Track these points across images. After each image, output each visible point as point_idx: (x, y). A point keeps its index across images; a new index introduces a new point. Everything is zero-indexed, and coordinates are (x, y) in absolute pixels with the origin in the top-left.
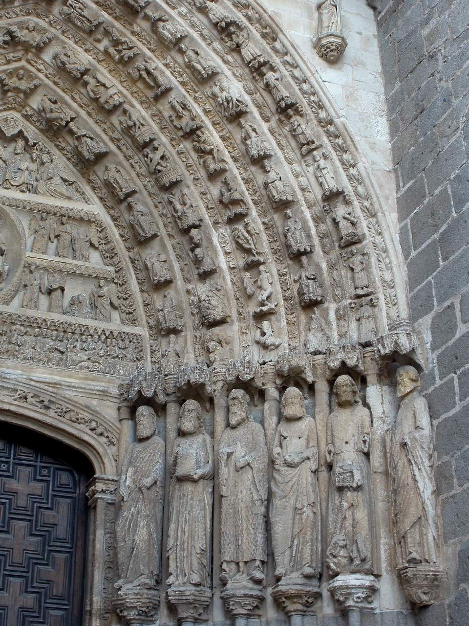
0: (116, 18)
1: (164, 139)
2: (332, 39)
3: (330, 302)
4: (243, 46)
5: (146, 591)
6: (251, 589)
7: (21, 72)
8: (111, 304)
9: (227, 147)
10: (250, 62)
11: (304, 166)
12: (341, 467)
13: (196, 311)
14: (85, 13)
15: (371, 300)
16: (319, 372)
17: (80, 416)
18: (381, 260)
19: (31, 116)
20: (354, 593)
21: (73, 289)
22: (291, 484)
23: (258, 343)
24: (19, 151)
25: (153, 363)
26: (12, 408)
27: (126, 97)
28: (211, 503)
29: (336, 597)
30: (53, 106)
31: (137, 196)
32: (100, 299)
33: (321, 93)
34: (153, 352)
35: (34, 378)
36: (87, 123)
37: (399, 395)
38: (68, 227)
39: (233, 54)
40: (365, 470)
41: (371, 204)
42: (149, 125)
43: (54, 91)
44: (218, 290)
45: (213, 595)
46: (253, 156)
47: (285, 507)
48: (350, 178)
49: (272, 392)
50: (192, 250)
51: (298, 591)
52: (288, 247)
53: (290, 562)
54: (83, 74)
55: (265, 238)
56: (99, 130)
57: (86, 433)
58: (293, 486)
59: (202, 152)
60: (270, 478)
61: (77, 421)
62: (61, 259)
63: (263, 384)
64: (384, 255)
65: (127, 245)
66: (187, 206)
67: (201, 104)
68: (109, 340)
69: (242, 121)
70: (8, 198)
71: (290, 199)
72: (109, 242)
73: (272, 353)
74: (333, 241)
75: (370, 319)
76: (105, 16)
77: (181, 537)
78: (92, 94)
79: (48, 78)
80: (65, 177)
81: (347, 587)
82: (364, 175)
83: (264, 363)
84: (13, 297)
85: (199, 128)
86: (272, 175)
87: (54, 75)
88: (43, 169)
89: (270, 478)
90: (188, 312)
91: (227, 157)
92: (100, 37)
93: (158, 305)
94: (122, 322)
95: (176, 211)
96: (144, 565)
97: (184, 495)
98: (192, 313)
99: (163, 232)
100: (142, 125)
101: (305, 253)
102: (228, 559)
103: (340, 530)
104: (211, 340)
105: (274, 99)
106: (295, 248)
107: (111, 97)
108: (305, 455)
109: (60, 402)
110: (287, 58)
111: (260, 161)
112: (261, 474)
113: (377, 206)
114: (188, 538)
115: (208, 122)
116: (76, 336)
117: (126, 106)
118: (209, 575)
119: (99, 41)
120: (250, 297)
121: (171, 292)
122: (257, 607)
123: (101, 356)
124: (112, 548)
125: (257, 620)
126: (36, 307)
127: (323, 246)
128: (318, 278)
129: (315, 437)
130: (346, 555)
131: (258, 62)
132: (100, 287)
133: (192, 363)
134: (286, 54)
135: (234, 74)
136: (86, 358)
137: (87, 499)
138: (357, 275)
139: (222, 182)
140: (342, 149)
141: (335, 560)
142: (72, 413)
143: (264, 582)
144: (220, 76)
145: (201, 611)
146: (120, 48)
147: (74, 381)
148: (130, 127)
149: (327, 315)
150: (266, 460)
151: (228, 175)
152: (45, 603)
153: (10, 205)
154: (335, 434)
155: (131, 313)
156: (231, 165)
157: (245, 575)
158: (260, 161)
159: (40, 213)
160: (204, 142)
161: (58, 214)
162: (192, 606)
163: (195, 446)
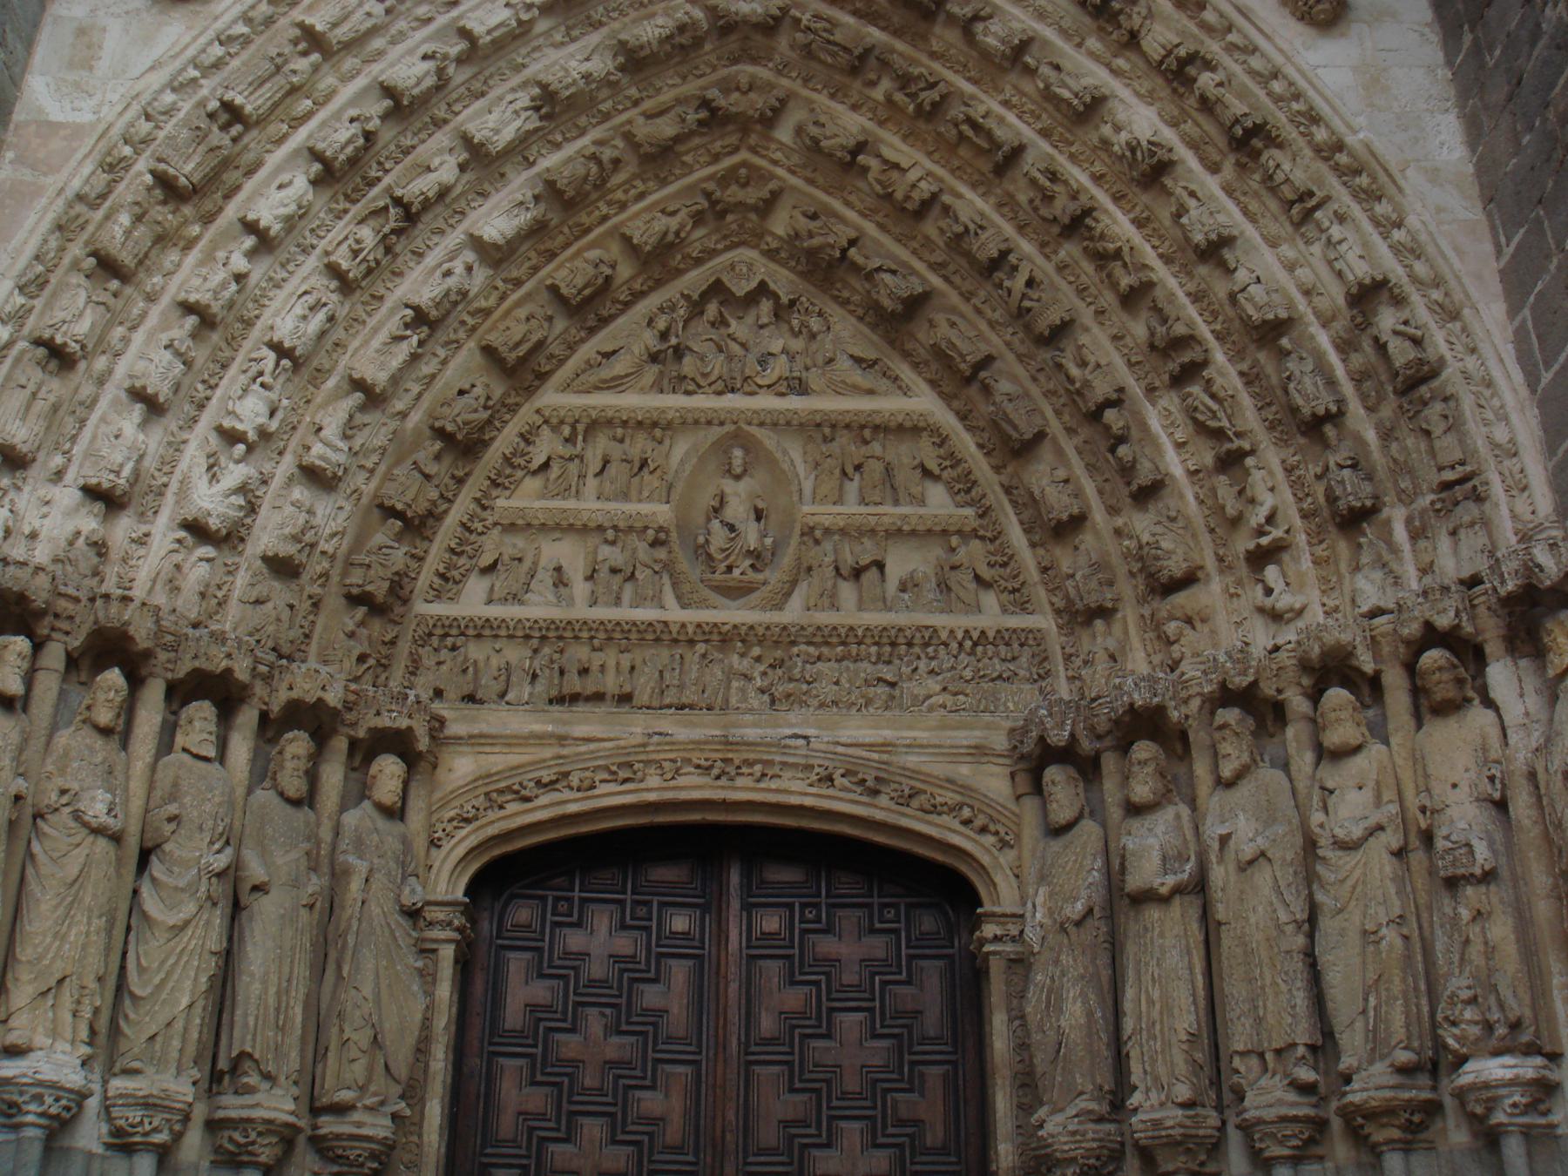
0: (897, 33)
1: (1026, 247)
3: (1392, 506)
4: (1143, 33)
5: (1091, 1126)
6: (1293, 1105)
7: (743, 171)
8: (977, 578)
9: (1147, 238)
10: (1161, 62)
11: (1301, 246)
12: (1447, 838)
13: (1136, 567)
14: (838, 37)
15: (1475, 488)
16: (1386, 649)
17: (939, 799)
18: (1483, 402)
19: (777, 250)
20: (1503, 1097)
21: (902, 562)
22: (1350, 883)
23: (1261, 610)
24: (765, 320)
25: (1071, 679)
26: (808, 801)
27: (941, 180)
28: (1201, 938)
29: (1469, 1108)
30: (813, 225)
31: (997, 365)
32: (953, 573)
33: (1311, 93)
34: (1068, 658)
35: (843, 740)
36: (882, 245)
37: (1551, 673)
38: (876, 447)
39: (1128, 54)
40: (1498, 837)
41: (1446, 294)
42: (994, 225)
43: (810, 196)
44: (1173, 520)
45: (1224, 1122)
46: (1197, 246)
47: (1342, 933)
48: (1397, 249)
49: (1297, 703)
50: (1113, 450)
51: (1387, 1100)
52: (1294, 410)
53: (1367, 1041)
55: (1246, 401)
56: (903, 254)
57: (954, 831)
58: (1354, 887)
59: (1104, 258)
60: (1310, 878)
61: (934, 810)
62: (872, 509)
63: (1279, 691)
64: (1487, 393)
65: (994, 461)
66: (1090, 368)
67: (1086, 165)
68: (980, 649)
69: (1168, 182)
70: (755, 412)
71: (1283, 314)
72: (959, 462)
73: (1292, 626)
74: (1382, 384)
75: (1477, 527)
76: (875, 34)
77: (1149, 1013)
78: (878, 188)
79: (793, 173)
80: (858, 352)
81: (1486, 1086)
82: (1423, 237)
83: (1276, 649)
84: (788, 595)
85: (1088, 212)
86: (1242, 276)
87: (804, 166)
88: (814, 346)
89: (1310, 878)
90: (1121, 570)
91: (1150, 256)
92: (872, 76)
93: (1065, 566)
94: (1004, 611)
95: (1071, 380)
96: (1082, 1075)
97: (1146, 929)
98: (1130, 572)
99: (1055, 427)
100: (981, 227)
101: (1329, 417)
102: (1240, 1047)
103: (1461, 966)
104: (1172, 618)
105: (1222, 125)
106: (1306, 411)
107: (914, 186)
108: (1372, 822)
109: (898, 778)
110: (1232, 37)
111: (1215, 251)
112: (1291, 870)
113: (1458, 296)
114: (1161, 1013)
115: (1102, 198)
116: (917, 650)
117: (946, 198)
118: (1211, 1083)
119: (873, 84)
120: (1236, 522)
121: (1087, 540)
122: (1311, 1141)
123: (967, 681)
124: (1023, 1046)
125: (1316, 1167)
126: (834, 606)
127: (1364, 397)
128: (1363, 463)
129: (1392, 781)
130: (1476, 1018)
131: (1178, 59)
132: (953, 550)
133: (1144, 669)
134: (1229, 29)
135: (1137, 94)
136: (938, 688)
137: (973, 956)
138: (1437, 444)
139: (1150, 308)
140: (1369, 196)
141: (1456, 1031)
142: (923, 797)
143: (1322, 1089)
144: (1111, 104)
145: (1203, 1157)
146: (913, 89)
147: (922, 735)
148: (959, 237)
149: (1390, 532)
150: (1299, 840)
151: (1158, 293)
152: (912, 1163)
153: (761, 424)
154: (1431, 770)
155: (1018, 590)
157: (1277, 1078)
158: (1215, 251)
159: (820, 429)
160: (1102, 237)
161: (855, 425)
162: (1181, 1149)
163: (1160, 829)
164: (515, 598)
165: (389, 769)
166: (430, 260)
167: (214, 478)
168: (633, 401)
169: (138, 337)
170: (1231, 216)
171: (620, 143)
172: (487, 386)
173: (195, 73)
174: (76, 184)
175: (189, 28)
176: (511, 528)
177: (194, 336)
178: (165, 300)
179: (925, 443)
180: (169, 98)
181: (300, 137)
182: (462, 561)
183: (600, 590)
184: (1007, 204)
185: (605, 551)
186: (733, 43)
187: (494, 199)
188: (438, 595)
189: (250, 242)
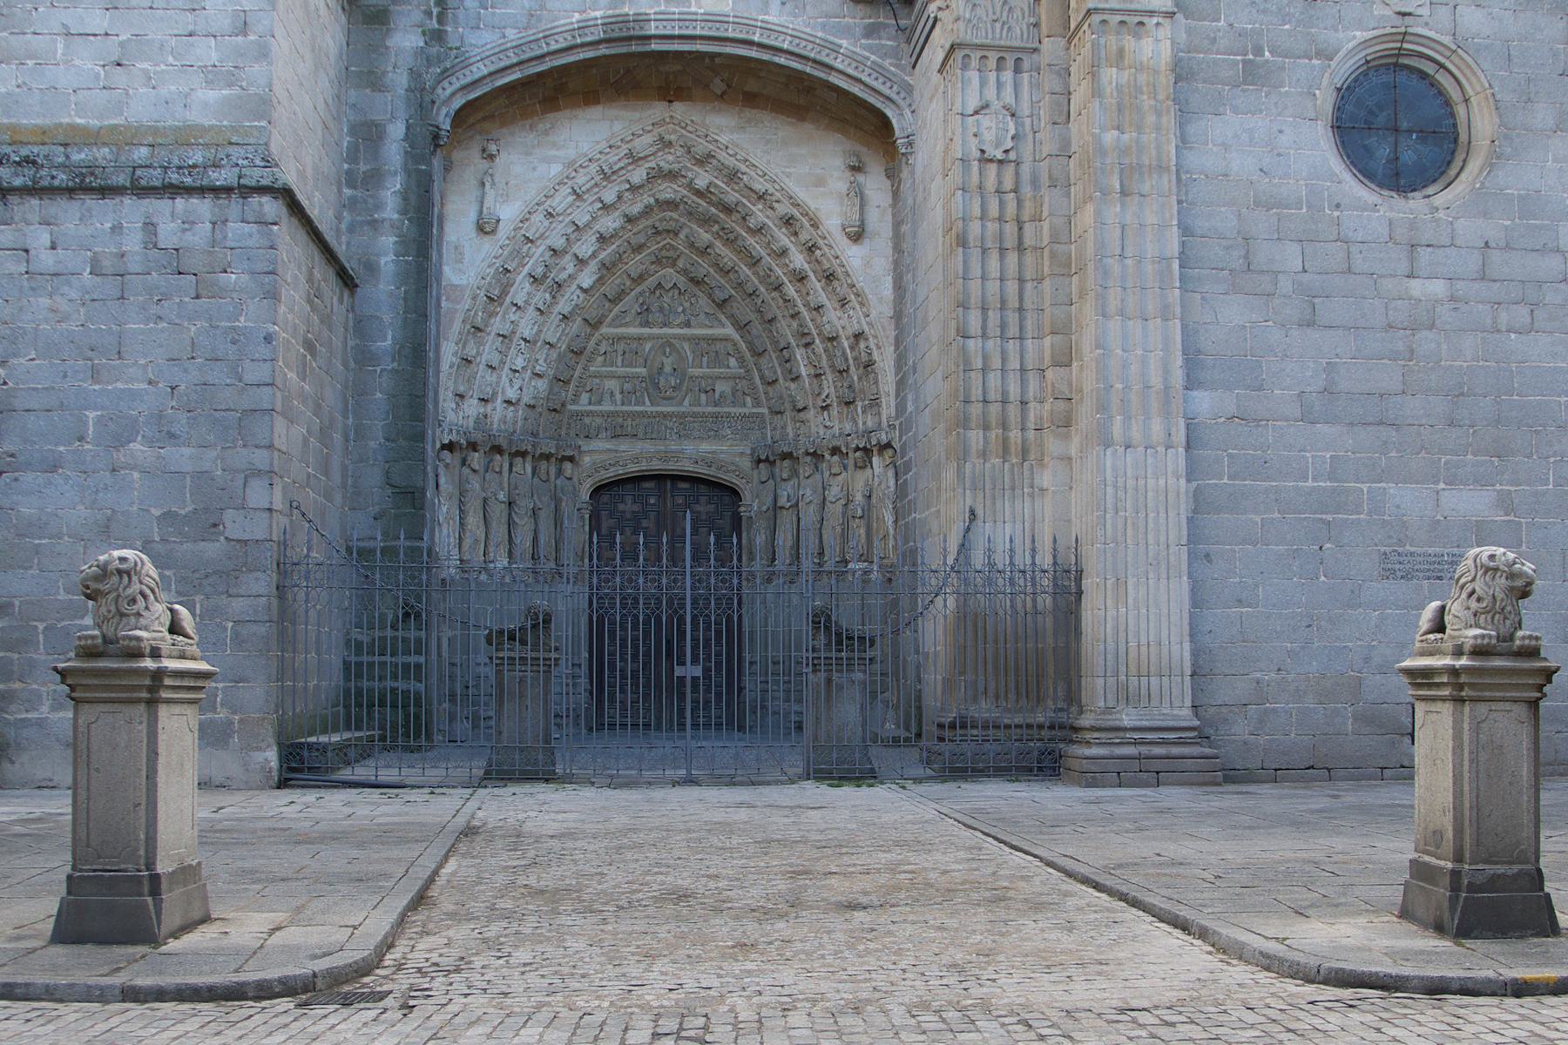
1: (762, 289)
2: (851, 229)
14: (700, 209)
21: (721, 387)
49: (827, 456)
55: (824, 356)
56: (723, 282)
86: (824, 318)
91: (799, 302)
93: (771, 393)
111: (818, 308)
140: (861, 304)
156: (802, 309)
158: (818, 308)
159: (695, 340)
164: (599, 403)
165: (568, 466)
166: (566, 297)
167: (511, 385)
169: (487, 347)
170: (823, 298)
172: (586, 332)
174: (467, 307)
176: (595, 377)
177: (502, 342)
180: (488, 271)
181: (526, 270)
182: (580, 389)
183: (626, 400)
184: (756, 273)
185: (626, 385)
188: (574, 402)
189: (515, 308)
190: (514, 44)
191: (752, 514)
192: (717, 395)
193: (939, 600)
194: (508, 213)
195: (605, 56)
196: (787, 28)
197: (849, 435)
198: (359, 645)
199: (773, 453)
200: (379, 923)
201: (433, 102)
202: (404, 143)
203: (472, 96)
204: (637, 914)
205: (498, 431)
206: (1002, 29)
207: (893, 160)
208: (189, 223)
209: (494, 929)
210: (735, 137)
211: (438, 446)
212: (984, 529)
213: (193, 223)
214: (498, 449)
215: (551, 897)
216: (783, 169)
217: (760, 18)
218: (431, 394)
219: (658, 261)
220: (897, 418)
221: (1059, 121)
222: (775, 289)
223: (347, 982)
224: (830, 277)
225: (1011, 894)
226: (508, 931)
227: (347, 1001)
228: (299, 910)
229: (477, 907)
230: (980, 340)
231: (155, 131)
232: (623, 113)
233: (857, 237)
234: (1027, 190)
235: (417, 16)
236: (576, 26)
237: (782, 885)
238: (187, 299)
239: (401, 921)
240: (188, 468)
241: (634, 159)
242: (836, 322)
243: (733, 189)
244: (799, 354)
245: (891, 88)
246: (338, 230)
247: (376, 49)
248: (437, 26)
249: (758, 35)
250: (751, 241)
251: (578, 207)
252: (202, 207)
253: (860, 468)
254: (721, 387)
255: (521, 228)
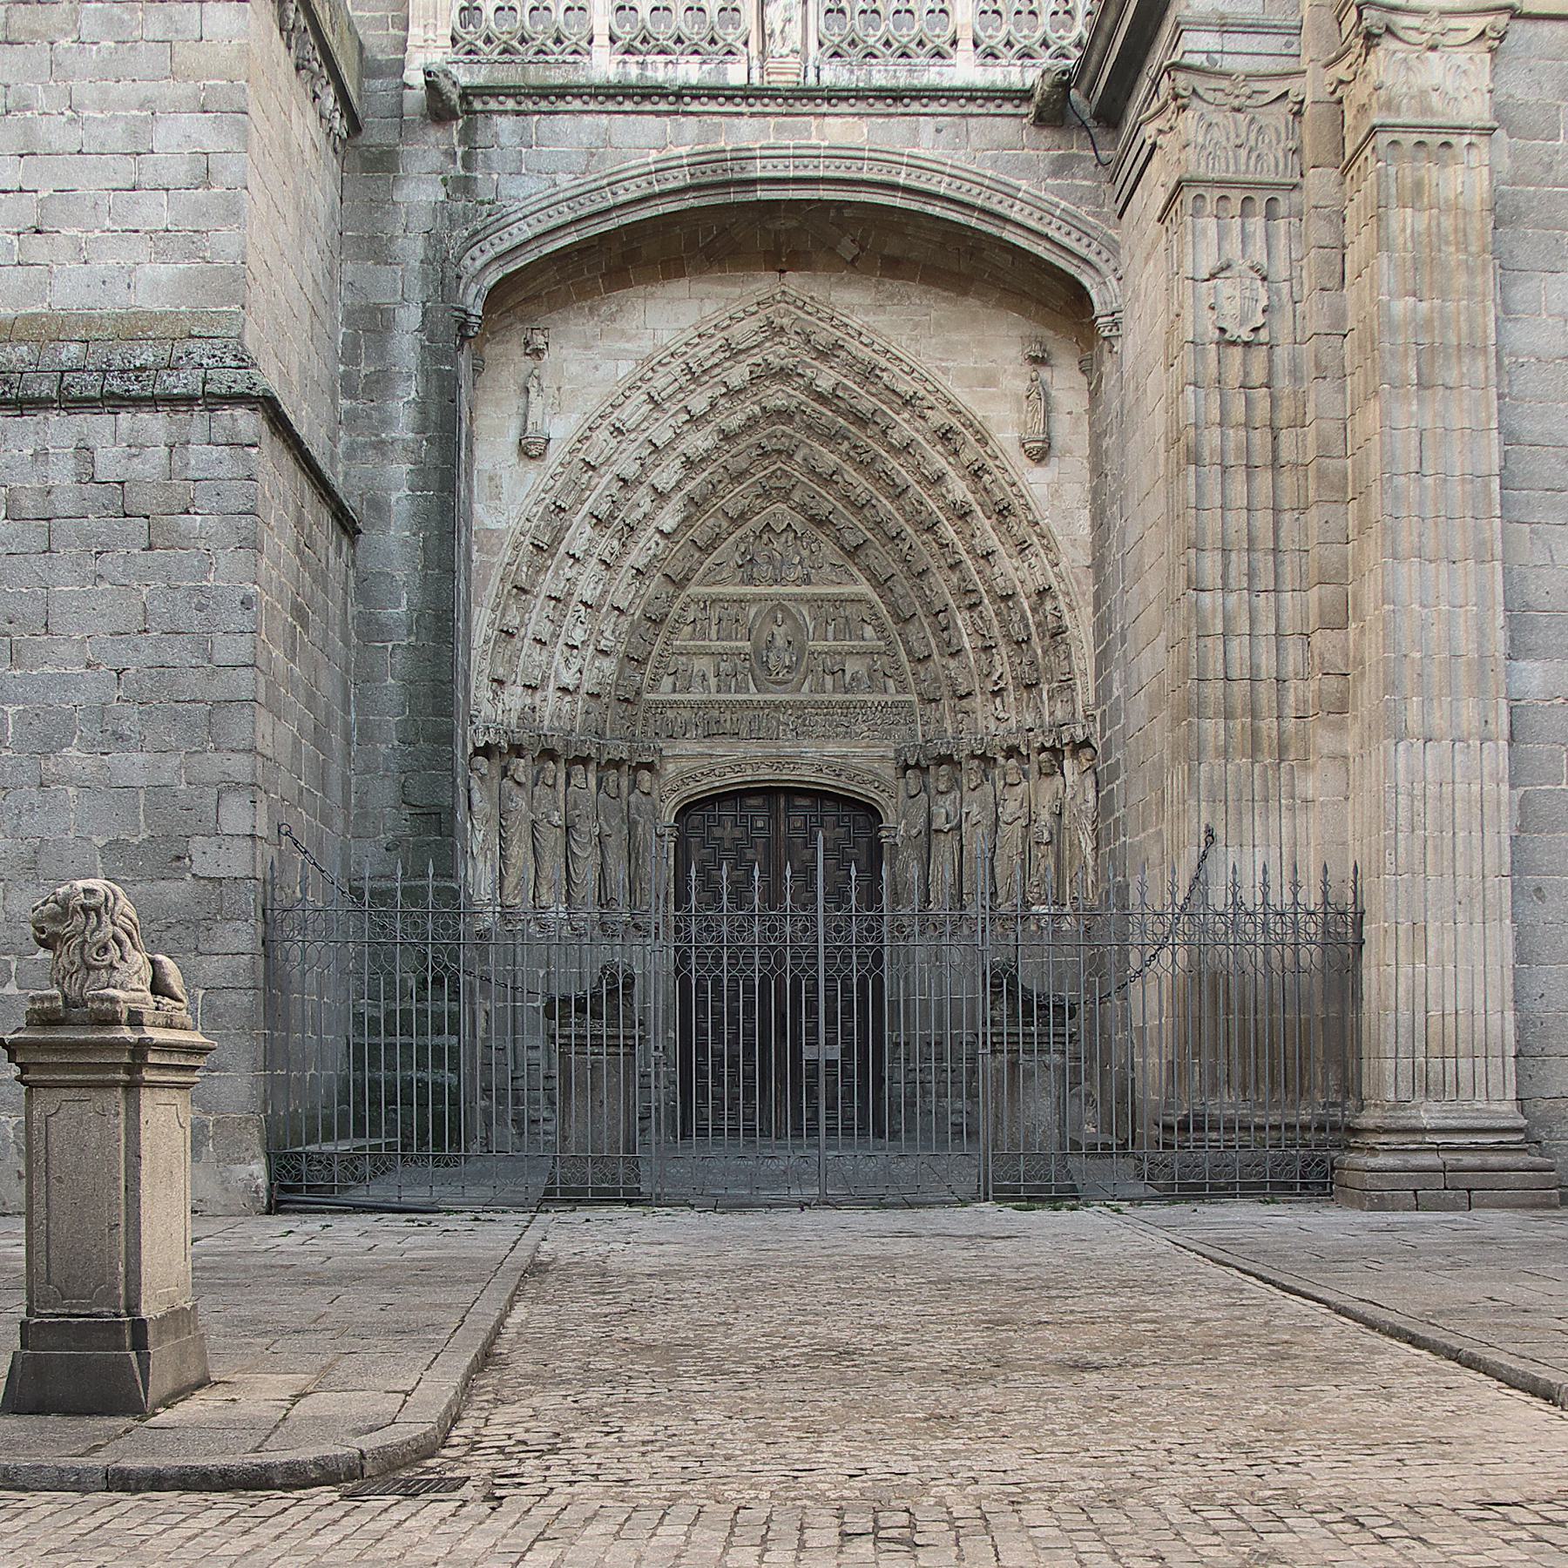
1: (909, 530)
2: (1032, 445)
14: (823, 421)
21: (853, 666)
26: (812, 779)
48: (1056, 575)
49: (1001, 760)
54: (831, 476)
55: (995, 623)
86: (996, 568)
91: (961, 550)
99: (920, 612)
110: (998, 463)
111: (987, 556)
115: (942, 518)
116: (858, 710)
117: (874, 502)
140: (1047, 548)
146: (859, 450)
151: (963, 565)
156: (965, 557)
159: (816, 601)
164: (687, 689)
165: (645, 775)
166: (641, 545)
168: (730, 589)
169: (534, 615)
170: (994, 542)
171: (721, 470)
173: (543, 495)
174: (506, 560)
175: (539, 474)
178: (542, 597)
179: (864, 607)
180: (535, 510)
181: (586, 508)
182: (661, 671)
183: (722, 685)
184: (900, 509)
186: (774, 418)
187: (665, 510)
188: (652, 689)
190: (568, 194)
191: (898, 840)
192: (848, 677)
193: (1165, 954)
194: (561, 429)
195: (692, 209)
196: (945, 164)
197: (1031, 730)
198: (374, 1021)
199: (925, 756)
200: (440, 1387)
201: (459, 277)
202: (420, 335)
203: (511, 268)
204: (785, 1377)
205: (551, 729)
206: (1249, 158)
207: (1091, 348)
208: (136, 447)
209: (593, 1397)
210: (870, 319)
211: (470, 750)
212: (1224, 858)
213: (143, 446)
214: (550, 754)
215: (668, 1354)
216: (938, 363)
217: (907, 151)
218: (460, 679)
219: (765, 494)
220: (1097, 705)
221: (1329, 286)
222: (928, 530)
223: (405, 1465)
224: (1003, 512)
225: (1296, 1350)
226: (612, 1399)
227: (410, 1491)
228: (326, 1370)
229: (567, 1367)
230: (1219, 594)
231: (89, 322)
232: (718, 289)
233: (1041, 454)
234: (1283, 383)
235: (435, 158)
236: (653, 168)
237: (978, 1339)
238: (136, 551)
239: (467, 1387)
240: (142, 782)
241: (733, 352)
242: (1011, 571)
243: (868, 392)
244: (962, 618)
245: (1089, 246)
246: (333, 456)
247: (380, 205)
248: (462, 173)
249: (903, 175)
250: (894, 463)
251: (657, 420)
252: (154, 423)
253: (1047, 775)
254: (853, 666)
255: (579, 450)
